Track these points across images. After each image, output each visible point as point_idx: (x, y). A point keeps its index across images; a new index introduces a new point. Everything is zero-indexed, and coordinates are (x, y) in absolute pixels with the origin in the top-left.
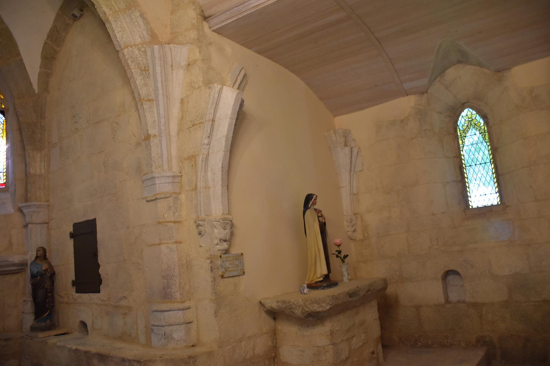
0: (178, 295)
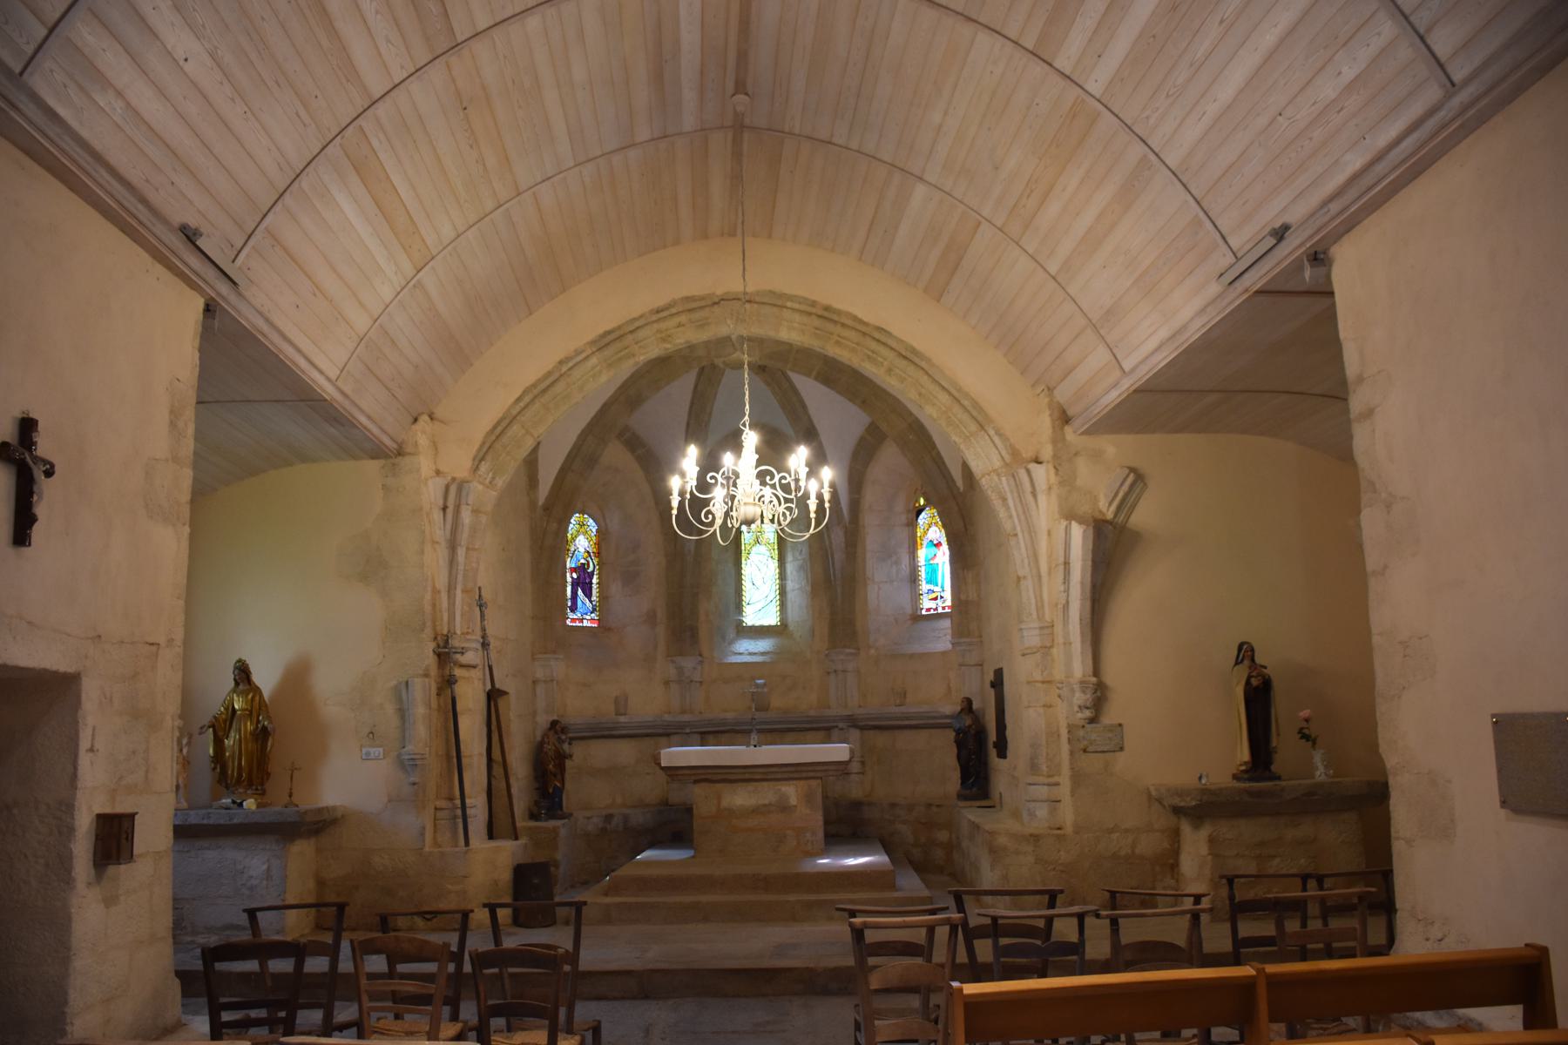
0: (1044, 768)
